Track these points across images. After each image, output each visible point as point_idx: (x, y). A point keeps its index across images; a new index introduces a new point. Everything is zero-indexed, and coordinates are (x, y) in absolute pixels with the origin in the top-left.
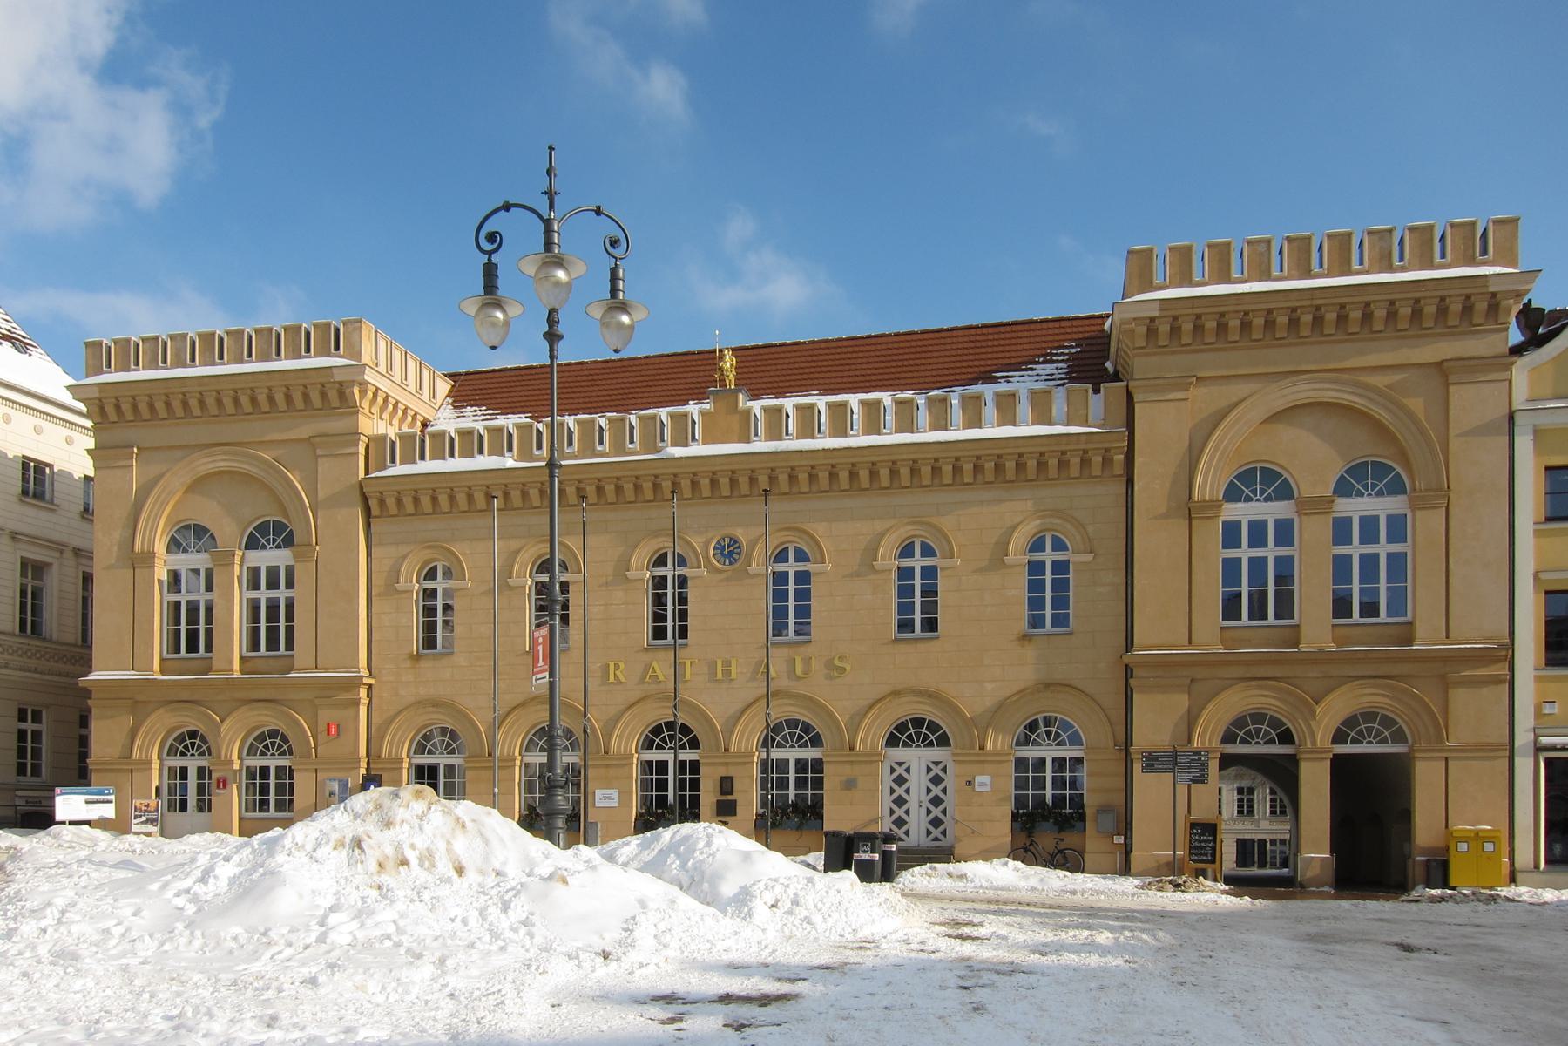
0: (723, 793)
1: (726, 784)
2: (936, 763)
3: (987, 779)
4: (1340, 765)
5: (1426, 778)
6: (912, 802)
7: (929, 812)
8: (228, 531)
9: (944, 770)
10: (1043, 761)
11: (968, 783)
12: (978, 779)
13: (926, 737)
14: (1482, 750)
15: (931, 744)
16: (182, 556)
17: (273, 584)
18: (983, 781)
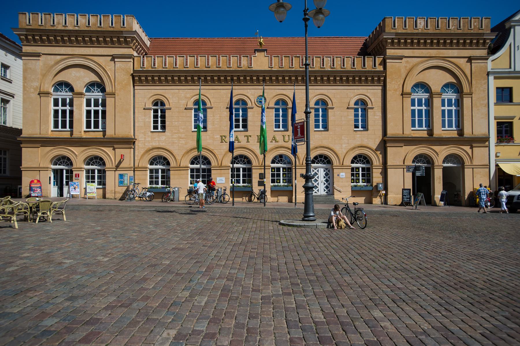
0: (260, 179)
1: (262, 176)
2: (327, 169)
3: (344, 174)
4: (445, 169)
5: (468, 172)
6: (319, 181)
7: (325, 184)
8: (79, 86)
9: (329, 171)
10: (358, 168)
11: (338, 175)
12: (341, 174)
13: (323, 161)
14: (483, 166)
15: (325, 163)
16: (59, 93)
17: (96, 105)
18: (343, 175)
